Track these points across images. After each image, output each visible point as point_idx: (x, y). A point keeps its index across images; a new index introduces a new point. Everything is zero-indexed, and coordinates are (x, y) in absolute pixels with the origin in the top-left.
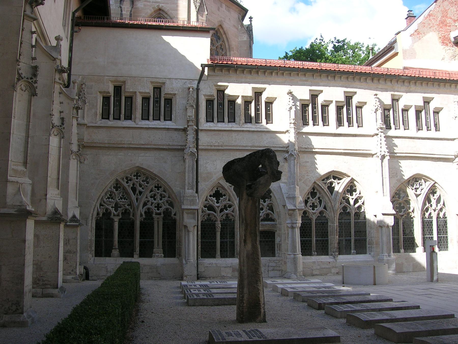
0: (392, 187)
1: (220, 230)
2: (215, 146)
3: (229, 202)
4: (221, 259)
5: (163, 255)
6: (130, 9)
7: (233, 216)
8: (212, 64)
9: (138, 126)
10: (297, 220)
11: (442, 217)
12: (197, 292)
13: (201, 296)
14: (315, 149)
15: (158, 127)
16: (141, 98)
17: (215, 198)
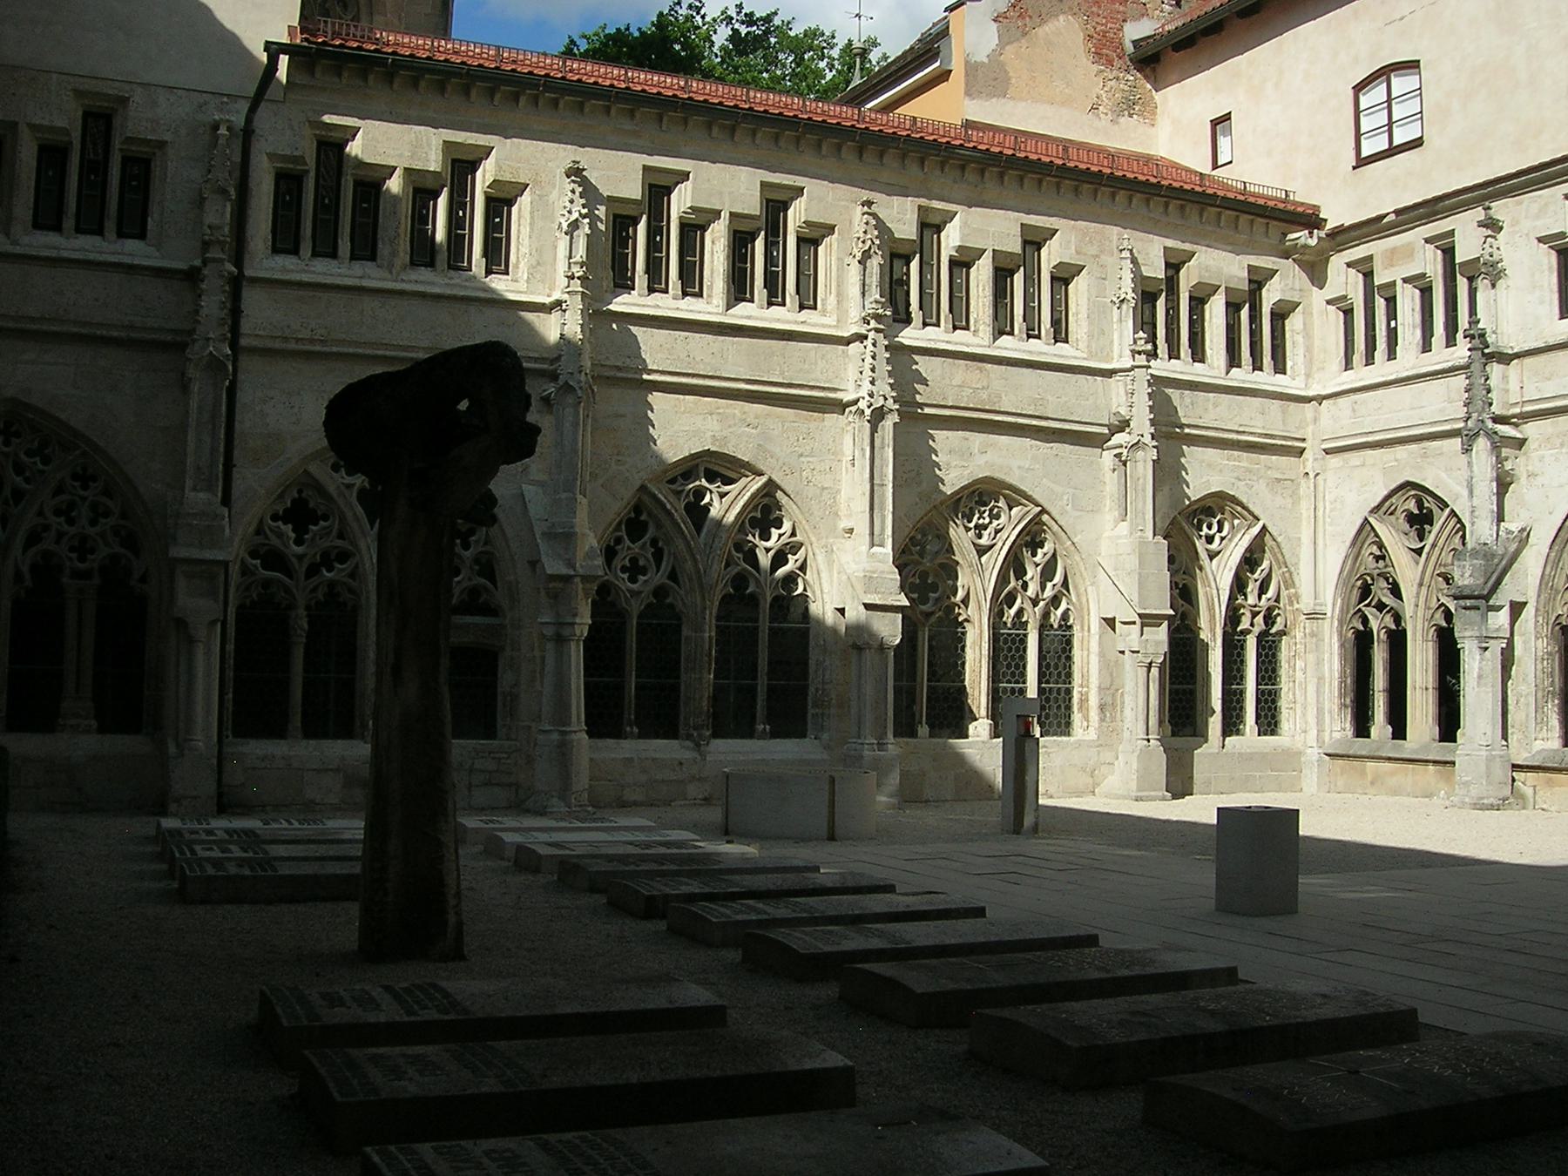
0: (900, 518)
1: (304, 640)
2: (298, 340)
3: (339, 543)
4: (304, 742)
5: (94, 724)
7: (351, 590)
8: (306, 44)
9: (18, 250)
10: (575, 615)
11: (1056, 626)
12: (216, 854)
13: (233, 870)
14: (651, 372)
15: (91, 256)
16: (36, 148)
17: (290, 526)
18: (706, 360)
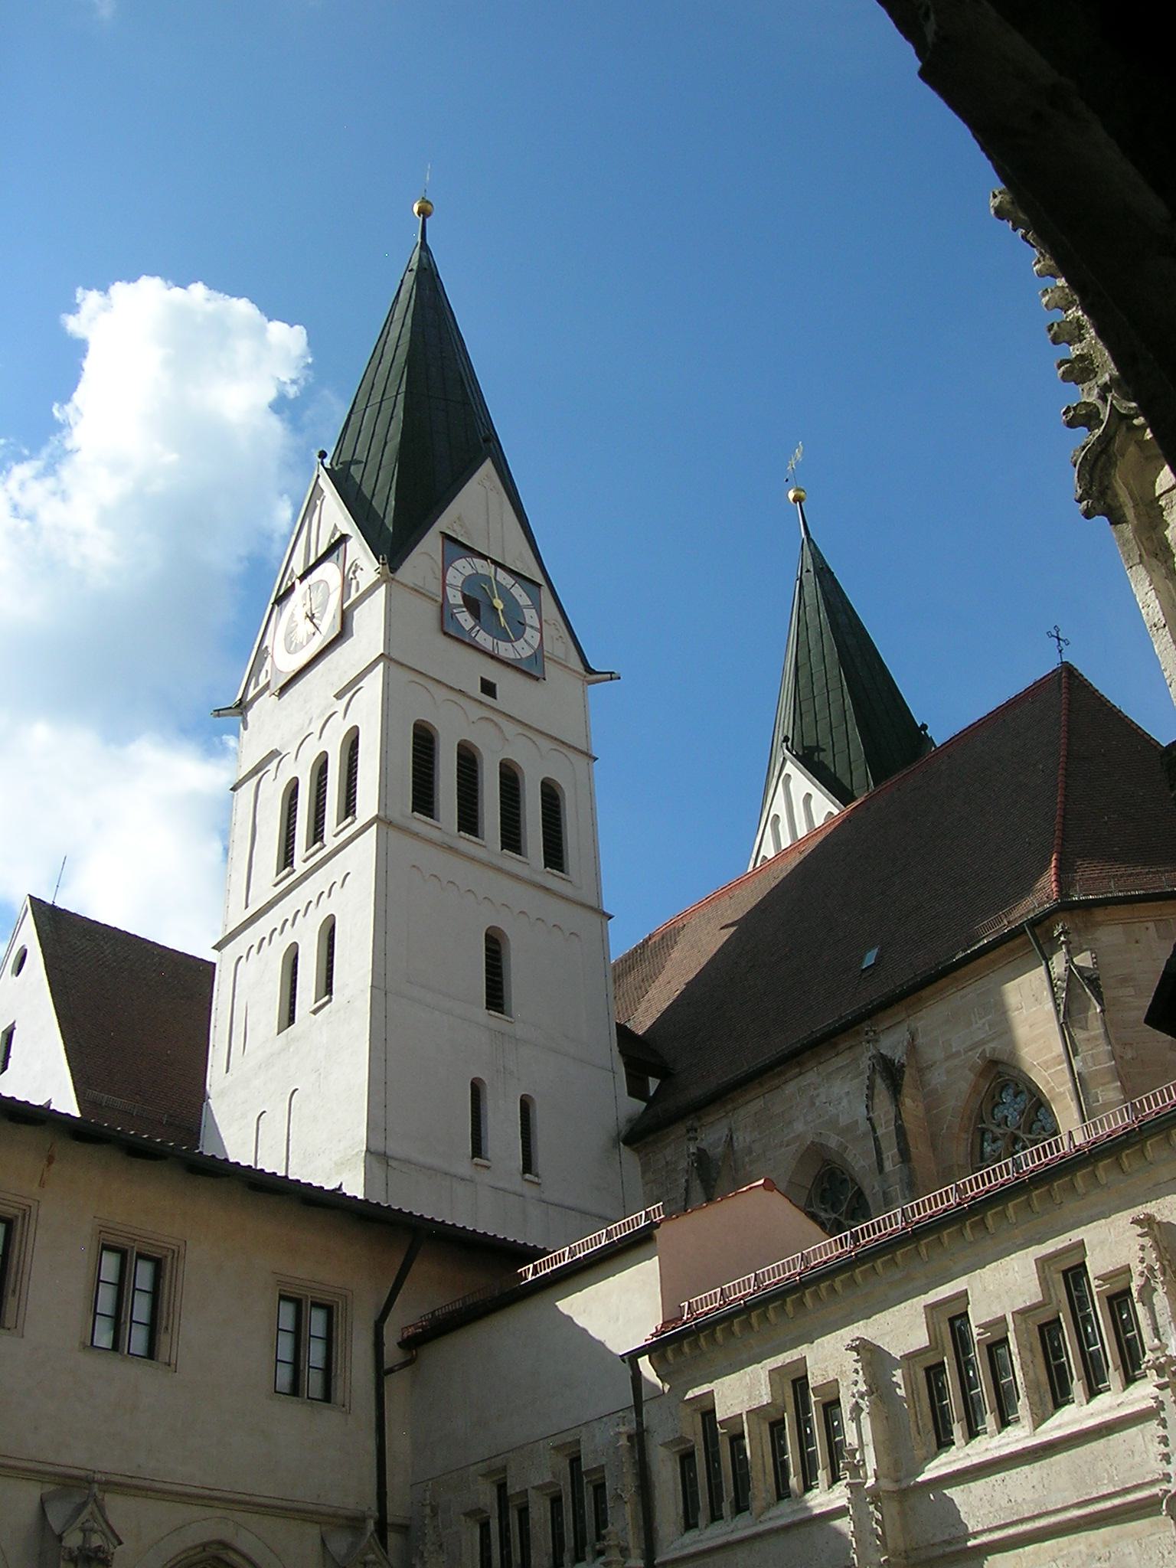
6: (892, 1115)
14: (975, 1535)
18: (1028, 1498)
